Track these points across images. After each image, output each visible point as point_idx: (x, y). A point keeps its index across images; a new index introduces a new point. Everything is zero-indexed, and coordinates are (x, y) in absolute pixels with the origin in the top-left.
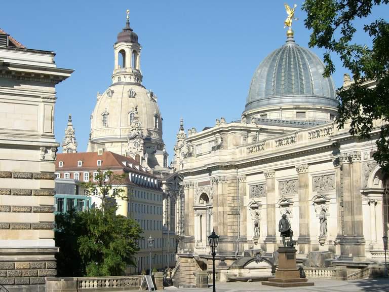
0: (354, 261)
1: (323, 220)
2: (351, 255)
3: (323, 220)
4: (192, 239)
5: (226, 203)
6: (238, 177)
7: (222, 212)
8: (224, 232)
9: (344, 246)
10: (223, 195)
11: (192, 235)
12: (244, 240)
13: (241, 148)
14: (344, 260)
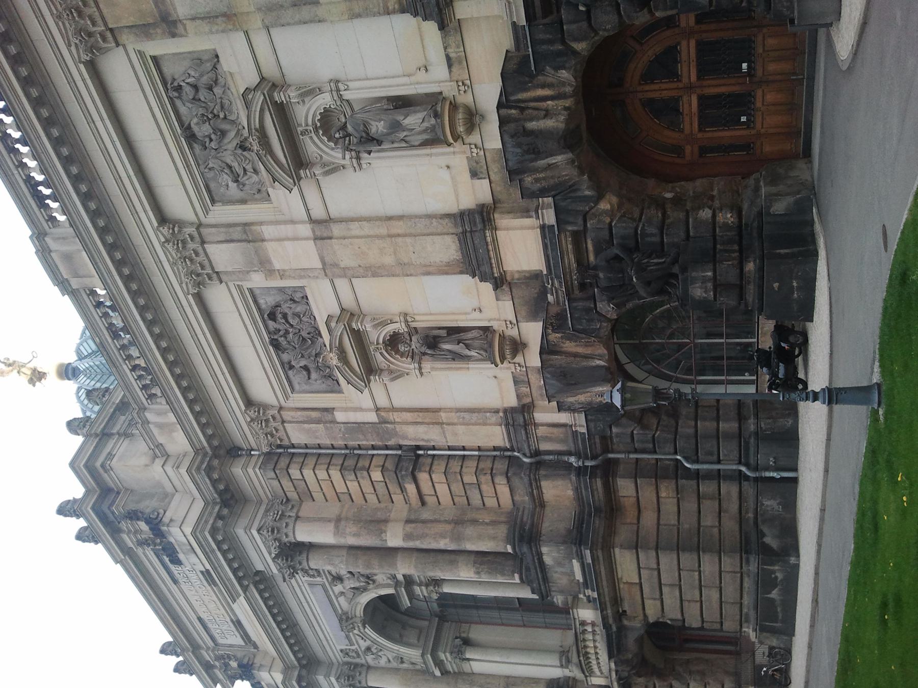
5: (377, 509)
6: (265, 449)
7: (409, 528)
8: (493, 523)
10: (338, 520)
12: (518, 418)
13: (155, 431)
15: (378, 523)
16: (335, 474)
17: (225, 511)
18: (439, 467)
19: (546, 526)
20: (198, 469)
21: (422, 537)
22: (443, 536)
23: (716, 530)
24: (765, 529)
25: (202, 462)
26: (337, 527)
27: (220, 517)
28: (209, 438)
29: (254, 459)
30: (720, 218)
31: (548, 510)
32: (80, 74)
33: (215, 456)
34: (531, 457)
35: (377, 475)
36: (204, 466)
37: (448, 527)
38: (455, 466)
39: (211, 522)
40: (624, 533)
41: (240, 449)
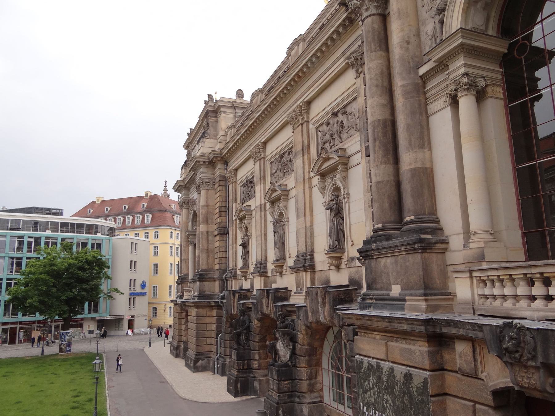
0: (406, 314)
1: (337, 210)
2: (396, 290)
3: (337, 210)
4: (185, 278)
5: (212, 219)
6: (226, 176)
7: (205, 233)
8: (208, 263)
9: (373, 263)
10: (207, 206)
11: (186, 272)
14: (376, 307)
15: (207, 221)
16: (218, 205)
17: (207, 163)
18: (223, 243)
19: (206, 283)
20: (214, 154)
21: (202, 239)
22: (202, 245)
23: (205, 343)
24: (205, 360)
25: (217, 154)
26: (204, 206)
27: (204, 162)
28: (225, 155)
29: (223, 172)
30: (256, 362)
31: (213, 282)
32: (283, 120)
33: (222, 158)
34: (225, 278)
35: (219, 220)
36: (216, 156)
37: (206, 247)
38: (223, 249)
39: (201, 160)
40: (203, 311)
41: (227, 165)
